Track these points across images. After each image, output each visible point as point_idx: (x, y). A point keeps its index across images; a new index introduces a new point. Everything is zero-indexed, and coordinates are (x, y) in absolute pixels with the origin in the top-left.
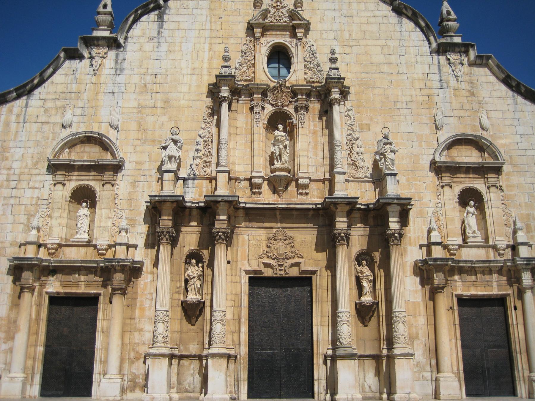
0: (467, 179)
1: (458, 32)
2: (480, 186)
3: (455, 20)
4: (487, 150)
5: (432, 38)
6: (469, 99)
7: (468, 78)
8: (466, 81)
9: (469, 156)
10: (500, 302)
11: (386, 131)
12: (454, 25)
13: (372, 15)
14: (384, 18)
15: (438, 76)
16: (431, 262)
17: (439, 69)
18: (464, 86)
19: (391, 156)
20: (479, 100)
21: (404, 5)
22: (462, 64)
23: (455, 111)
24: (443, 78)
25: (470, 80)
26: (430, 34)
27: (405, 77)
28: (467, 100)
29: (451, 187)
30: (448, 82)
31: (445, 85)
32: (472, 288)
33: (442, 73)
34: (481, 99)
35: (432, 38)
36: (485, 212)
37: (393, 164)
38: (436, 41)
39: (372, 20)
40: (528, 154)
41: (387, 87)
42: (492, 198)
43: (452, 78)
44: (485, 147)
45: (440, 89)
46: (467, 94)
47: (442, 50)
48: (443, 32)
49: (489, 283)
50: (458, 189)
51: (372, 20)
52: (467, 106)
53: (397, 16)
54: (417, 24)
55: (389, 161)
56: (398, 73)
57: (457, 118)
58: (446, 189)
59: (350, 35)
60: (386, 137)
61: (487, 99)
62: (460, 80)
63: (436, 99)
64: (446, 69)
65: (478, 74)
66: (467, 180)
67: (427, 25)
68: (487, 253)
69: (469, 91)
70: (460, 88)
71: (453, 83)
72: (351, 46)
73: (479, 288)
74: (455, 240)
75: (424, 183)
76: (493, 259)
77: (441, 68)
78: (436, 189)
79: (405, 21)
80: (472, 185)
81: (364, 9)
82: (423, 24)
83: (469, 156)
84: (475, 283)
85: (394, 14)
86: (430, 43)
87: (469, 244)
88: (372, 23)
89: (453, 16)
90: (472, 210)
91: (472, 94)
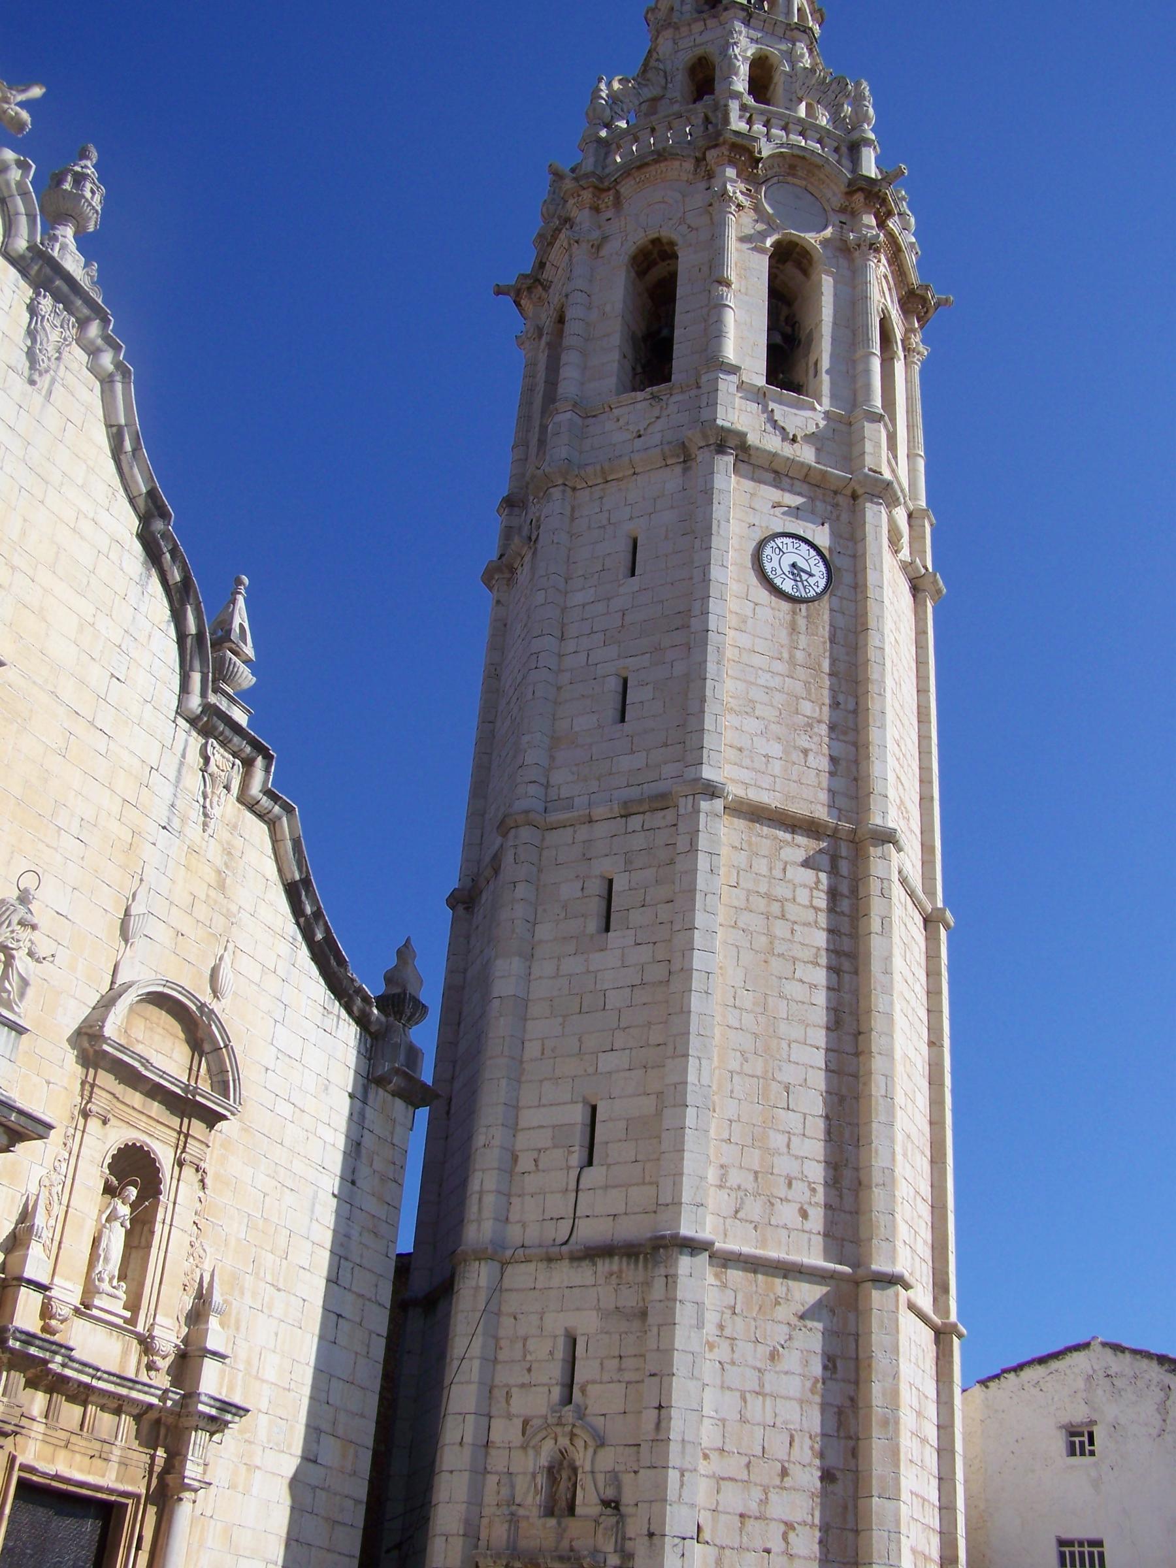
0: (144, 1118)
1: (245, 697)
2: (165, 1156)
3: (247, 662)
4: (210, 1057)
5: (196, 677)
6: (212, 893)
7: (225, 835)
8: (220, 842)
9: (167, 1055)
10: (105, 1513)
11: (29, 882)
12: (246, 677)
13: (91, 515)
14: (114, 544)
15: (172, 789)
16: (16, 1339)
17: (179, 771)
18: (213, 850)
19: (22, 962)
20: (228, 910)
21: (175, 546)
22: (227, 788)
23: (174, 909)
24: (178, 803)
25: (228, 843)
26: (197, 664)
27: (101, 743)
28: (208, 896)
29: (105, 1122)
30: (183, 821)
31: (176, 823)
32: (62, 1454)
33: (181, 786)
34: (234, 908)
35: (196, 677)
36: (152, 1233)
37: (22, 995)
38: (204, 694)
39: (86, 527)
40: (278, 1110)
41: (54, 746)
42: (180, 1196)
43: (196, 814)
44: (207, 1047)
45: (164, 828)
46: (212, 877)
47: (208, 724)
48: (220, 674)
49: (106, 1447)
50: (118, 1136)
51: (86, 527)
52: (201, 911)
53: (142, 559)
54: (178, 617)
55: (14, 978)
56: (92, 723)
57: (172, 933)
58: (94, 1124)
59: (24, 533)
60: (24, 898)
61: (244, 916)
62: (210, 831)
63: (147, 852)
64: (193, 781)
65: (247, 837)
66: (143, 1122)
67: (200, 636)
68: (125, 1353)
69: (219, 872)
70: (202, 852)
71: (194, 832)
72: (13, 568)
73: (78, 1457)
74: (68, 1292)
75: (48, 1083)
76: (131, 1374)
77: (184, 771)
78: (68, 1114)
79: (155, 585)
80: (148, 1140)
81: (80, 483)
82: (192, 628)
83: (167, 1055)
84: (74, 1439)
85: (137, 547)
86: (184, 688)
87: (95, 1312)
88: (82, 538)
89: (249, 650)
90: (124, 1210)
91: (222, 886)
